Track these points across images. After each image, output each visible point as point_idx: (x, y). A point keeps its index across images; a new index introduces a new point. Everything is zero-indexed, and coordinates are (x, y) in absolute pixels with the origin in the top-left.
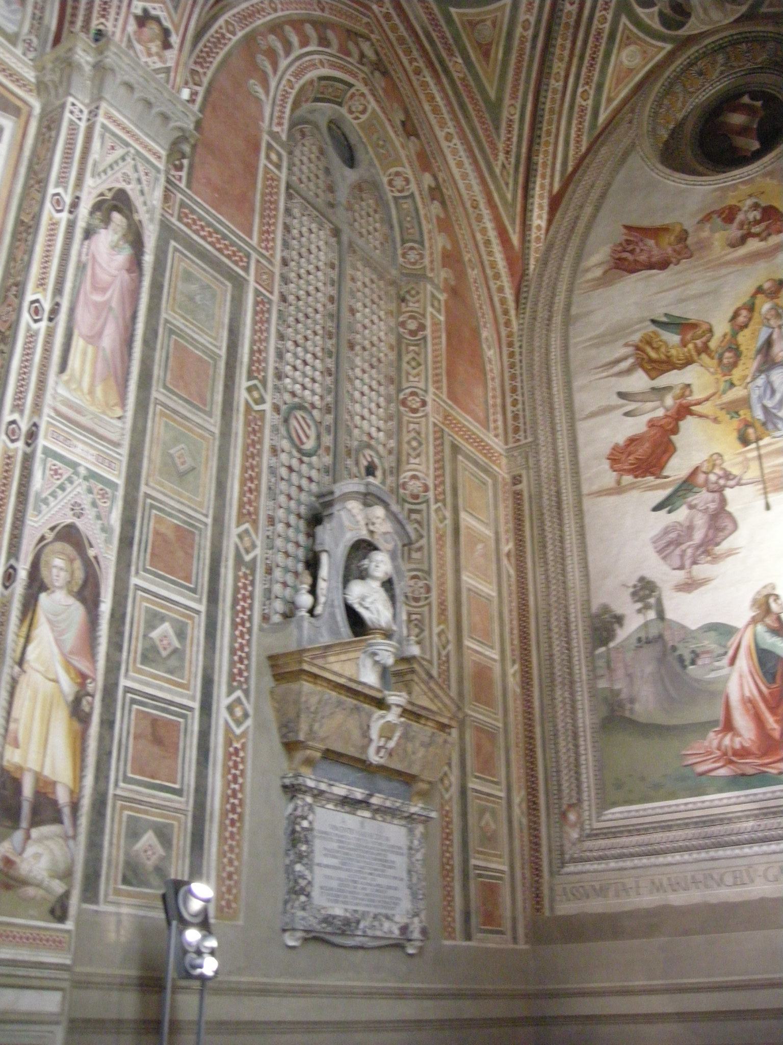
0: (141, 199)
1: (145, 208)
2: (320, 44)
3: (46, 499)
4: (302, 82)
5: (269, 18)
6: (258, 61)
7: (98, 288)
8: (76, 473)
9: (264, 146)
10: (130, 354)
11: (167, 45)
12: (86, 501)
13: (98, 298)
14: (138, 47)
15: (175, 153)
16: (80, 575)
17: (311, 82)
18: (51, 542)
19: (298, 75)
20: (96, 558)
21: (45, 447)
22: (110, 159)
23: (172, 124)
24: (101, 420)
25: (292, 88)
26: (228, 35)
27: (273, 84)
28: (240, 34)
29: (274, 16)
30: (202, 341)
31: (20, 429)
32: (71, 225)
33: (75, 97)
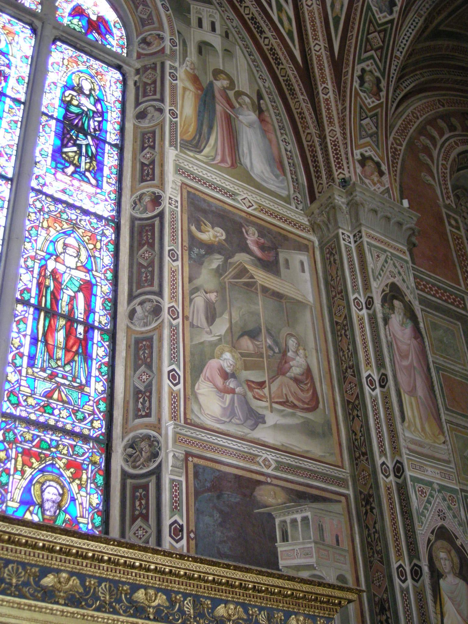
0: (405, 285)
1: (409, 291)
2: (451, 131)
3: (423, 512)
4: (450, 162)
5: (416, 125)
6: (421, 157)
7: (404, 356)
8: (433, 489)
9: (444, 216)
10: (435, 396)
11: (381, 174)
12: (444, 506)
13: (405, 363)
14: (367, 181)
15: (412, 247)
16: (456, 560)
17: (454, 160)
18: (434, 542)
19: (446, 159)
20: (462, 546)
21: (411, 476)
22: (379, 265)
23: (404, 227)
24: (434, 447)
25: (446, 169)
26: (399, 148)
27: (435, 171)
28: (404, 144)
29: (418, 122)
30: (457, 369)
31: (388, 467)
32: (373, 318)
33: (343, 229)
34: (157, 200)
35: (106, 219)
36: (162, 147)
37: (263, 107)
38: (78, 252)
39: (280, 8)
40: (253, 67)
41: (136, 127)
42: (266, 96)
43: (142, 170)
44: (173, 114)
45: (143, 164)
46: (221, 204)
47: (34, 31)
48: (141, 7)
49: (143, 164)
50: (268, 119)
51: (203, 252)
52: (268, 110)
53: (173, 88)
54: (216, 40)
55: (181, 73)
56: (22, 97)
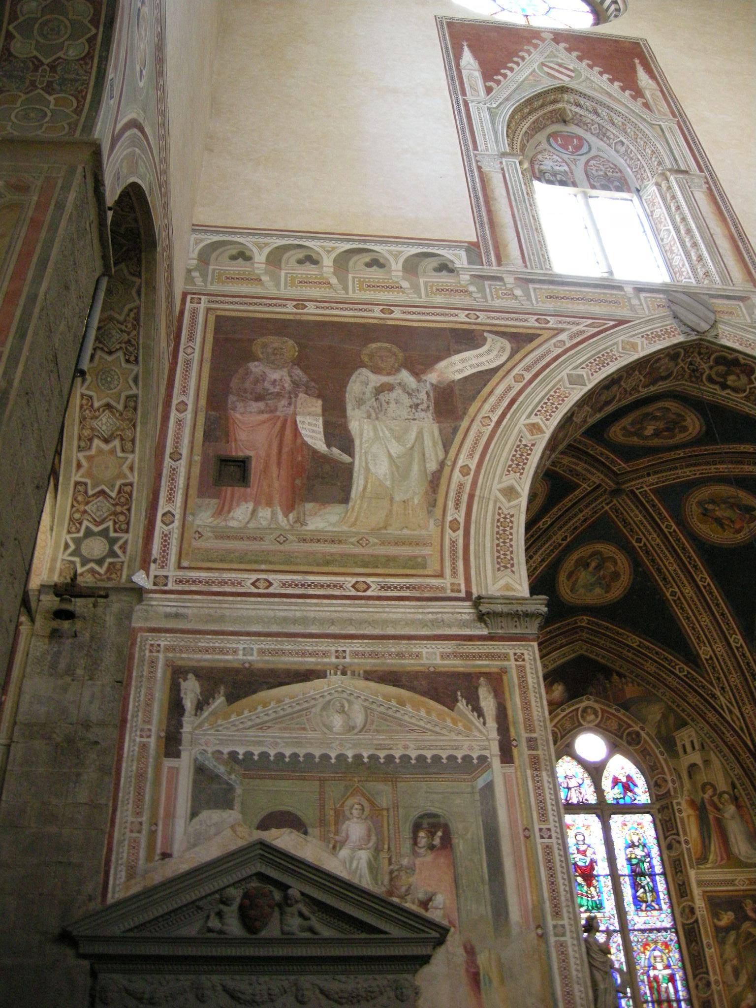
34: (692, 910)
35: (670, 929)
36: (687, 872)
37: (738, 794)
38: (661, 957)
39: (731, 712)
40: (725, 763)
41: (669, 857)
42: (738, 785)
43: (680, 890)
44: (687, 842)
45: (679, 885)
46: (727, 893)
47: (598, 816)
48: (648, 757)
49: (679, 885)
50: (743, 804)
51: (724, 934)
52: (741, 796)
53: (682, 819)
54: (696, 758)
55: (684, 806)
56: (607, 872)
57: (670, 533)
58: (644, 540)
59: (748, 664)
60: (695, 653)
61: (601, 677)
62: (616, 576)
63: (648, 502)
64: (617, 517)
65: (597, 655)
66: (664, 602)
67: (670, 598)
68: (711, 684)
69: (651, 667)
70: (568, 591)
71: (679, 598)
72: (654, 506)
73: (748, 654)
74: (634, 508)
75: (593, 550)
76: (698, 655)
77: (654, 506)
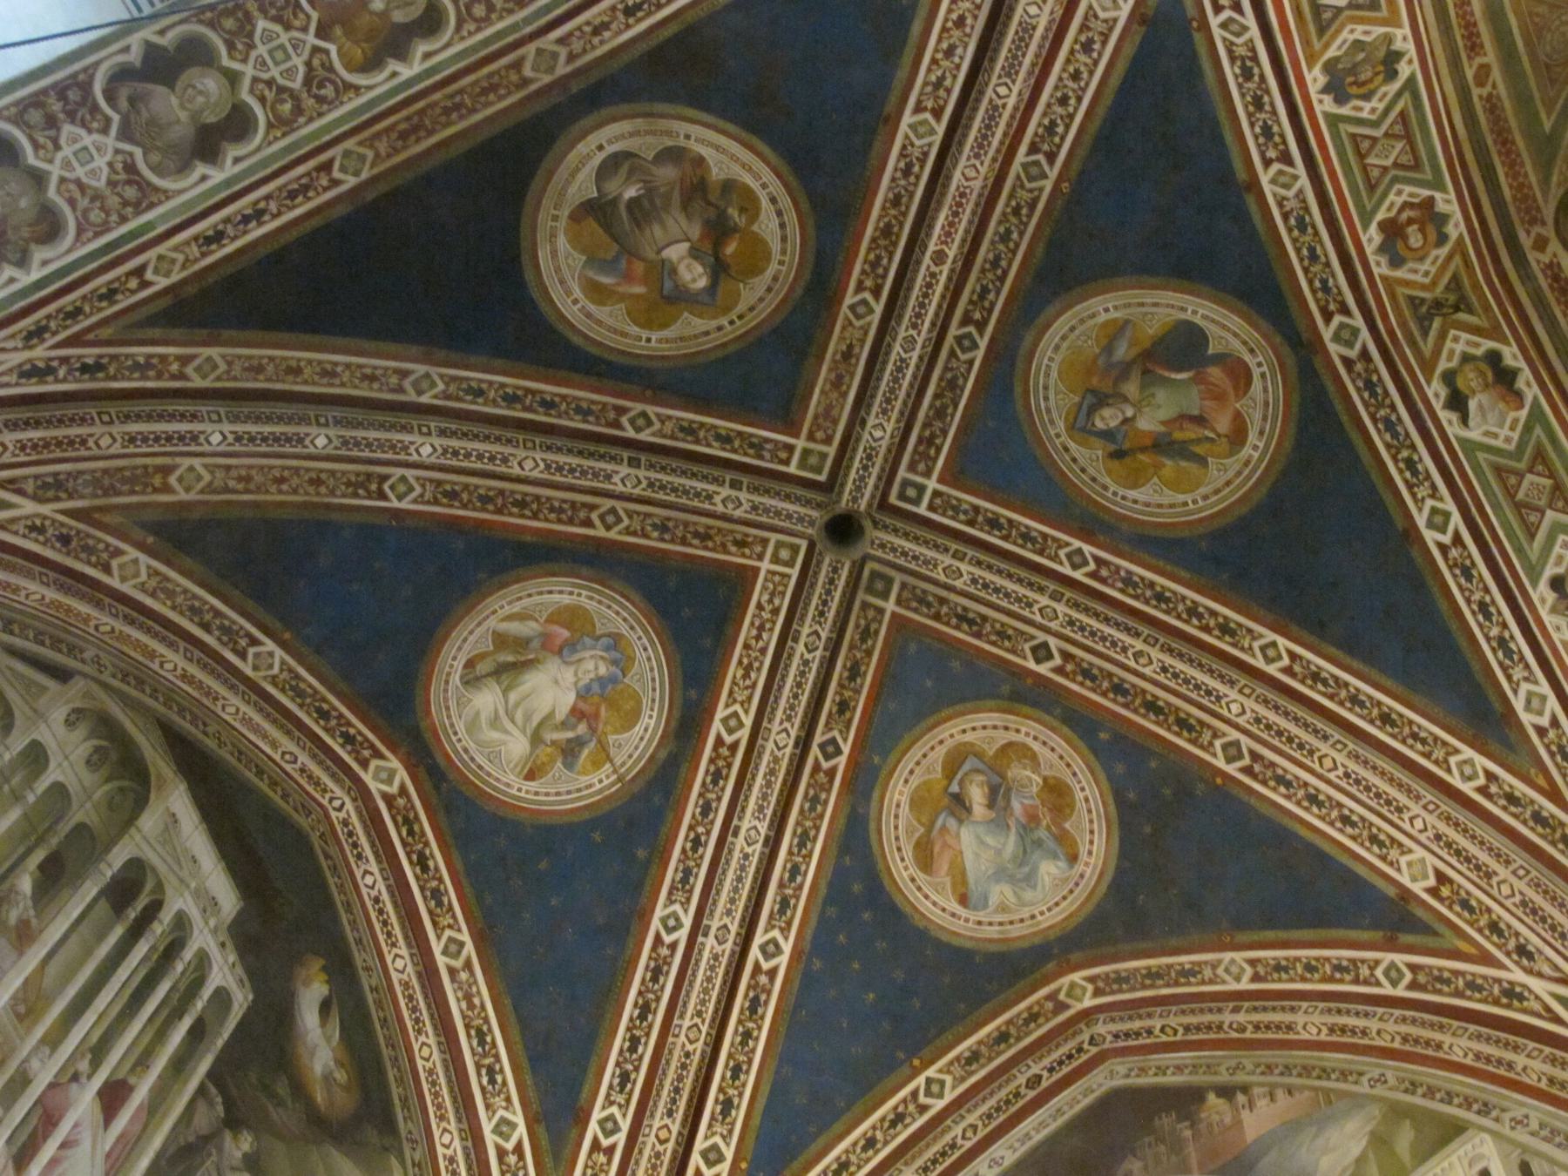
57: (1093, 575)
58: (1053, 642)
59: (1538, 818)
60: (1391, 892)
61: (1165, 1122)
62: (1057, 794)
63: (971, 523)
64: (937, 617)
65: (1162, 1071)
66: (1223, 793)
67: (1231, 769)
68: (1486, 959)
69: (1311, 1023)
70: (955, 906)
71: (1255, 756)
72: (994, 523)
73: (1521, 788)
74: (930, 554)
75: (941, 752)
76: (1406, 895)
77: (994, 523)
